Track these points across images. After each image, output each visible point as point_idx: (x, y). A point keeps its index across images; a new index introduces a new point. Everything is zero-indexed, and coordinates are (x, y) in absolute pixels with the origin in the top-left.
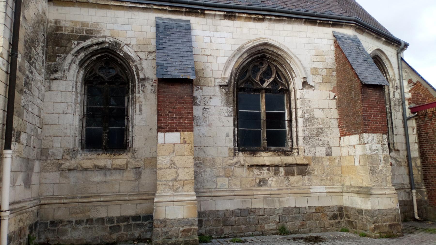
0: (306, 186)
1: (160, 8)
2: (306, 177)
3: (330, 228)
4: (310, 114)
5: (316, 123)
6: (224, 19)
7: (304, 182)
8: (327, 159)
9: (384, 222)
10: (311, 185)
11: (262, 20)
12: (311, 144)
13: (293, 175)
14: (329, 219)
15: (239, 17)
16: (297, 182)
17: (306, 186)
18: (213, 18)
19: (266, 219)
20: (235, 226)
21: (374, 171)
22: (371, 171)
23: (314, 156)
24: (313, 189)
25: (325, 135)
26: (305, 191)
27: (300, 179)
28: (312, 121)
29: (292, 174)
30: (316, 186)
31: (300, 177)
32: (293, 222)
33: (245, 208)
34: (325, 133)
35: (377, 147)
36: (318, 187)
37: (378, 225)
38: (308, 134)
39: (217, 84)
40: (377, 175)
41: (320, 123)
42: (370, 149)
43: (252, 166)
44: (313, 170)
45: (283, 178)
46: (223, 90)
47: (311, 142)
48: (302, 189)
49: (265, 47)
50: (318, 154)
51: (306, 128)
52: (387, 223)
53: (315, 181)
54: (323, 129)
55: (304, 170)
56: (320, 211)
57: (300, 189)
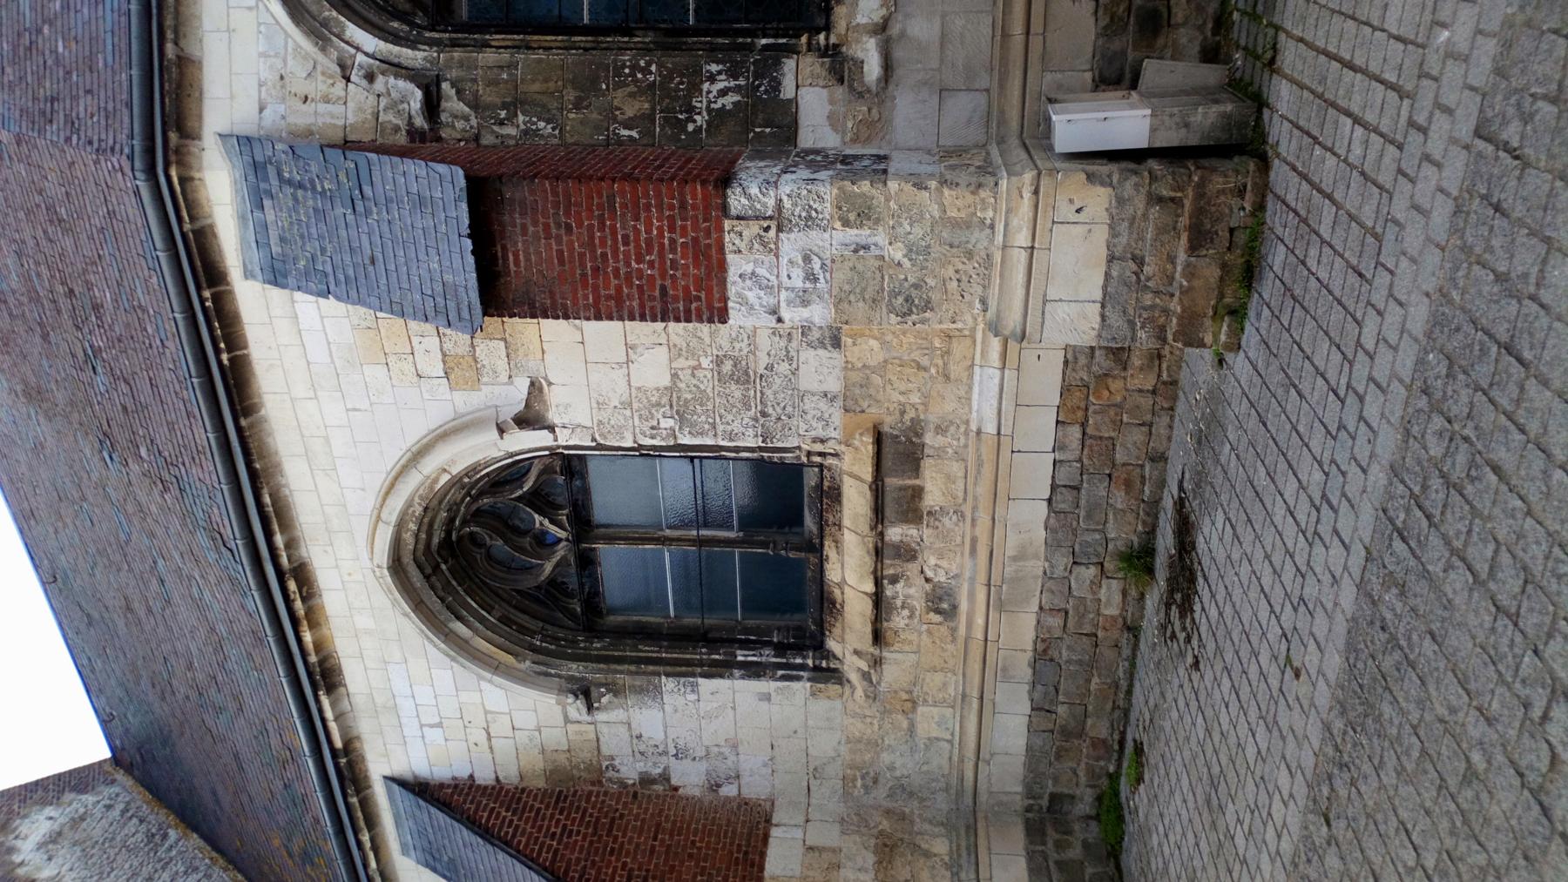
0: (966, 446)
1: (371, 856)
2: (929, 439)
3: (1164, 366)
4: (658, 404)
5: (695, 382)
6: (345, 686)
7: (950, 451)
8: (854, 344)
9: (1171, 279)
10: (967, 422)
11: (302, 573)
12: (789, 409)
13: (918, 492)
14: (1125, 369)
15: (318, 647)
16: (950, 478)
17: (966, 446)
18: (351, 715)
19: (1081, 609)
20: (1090, 708)
21: (914, 293)
22: (910, 313)
23: (839, 403)
24: (981, 420)
25: (744, 345)
26: (987, 452)
27: (935, 466)
28: (686, 401)
29: (913, 497)
30: (970, 409)
31: (928, 465)
32: (1111, 516)
33: (1029, 671)
34: (737, 346)
35: (791, 262)
36: (975, 396)
37: (1180, 318)
38: (746, 420)
39: (585, 717)
40: (931, 282)
41: (693, 363)
42: (805, 303)
43: (878, 637)
44: (903, 413)
45: (930, 531)
46: (604, 700)
47: (779, 410)
48: (980, 464)
49: (407, 559)
50: (834, 385)
51: (720, 428)
52: (1182, 257)
53: (949, 406)
54: (720, 353)
55: (901, 448)
56: (1083, 405)
57: (979, 472)
